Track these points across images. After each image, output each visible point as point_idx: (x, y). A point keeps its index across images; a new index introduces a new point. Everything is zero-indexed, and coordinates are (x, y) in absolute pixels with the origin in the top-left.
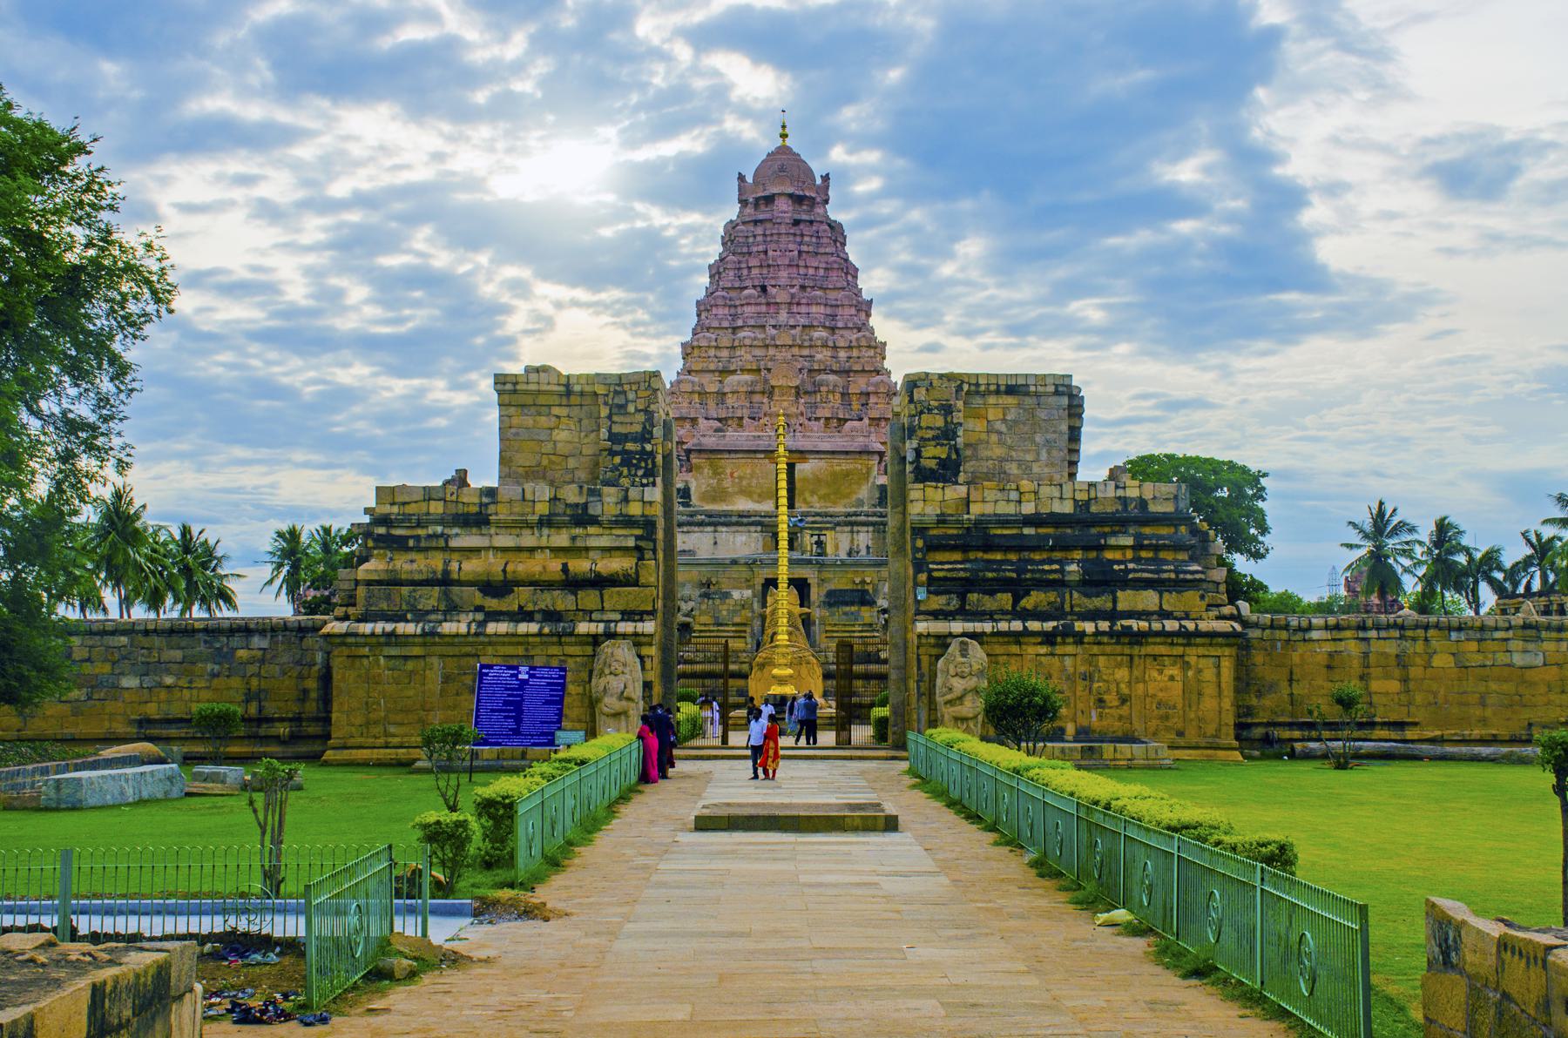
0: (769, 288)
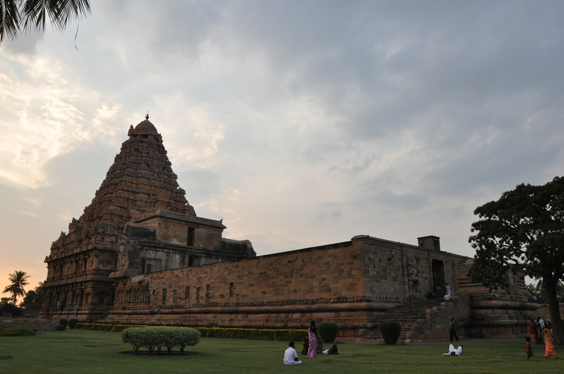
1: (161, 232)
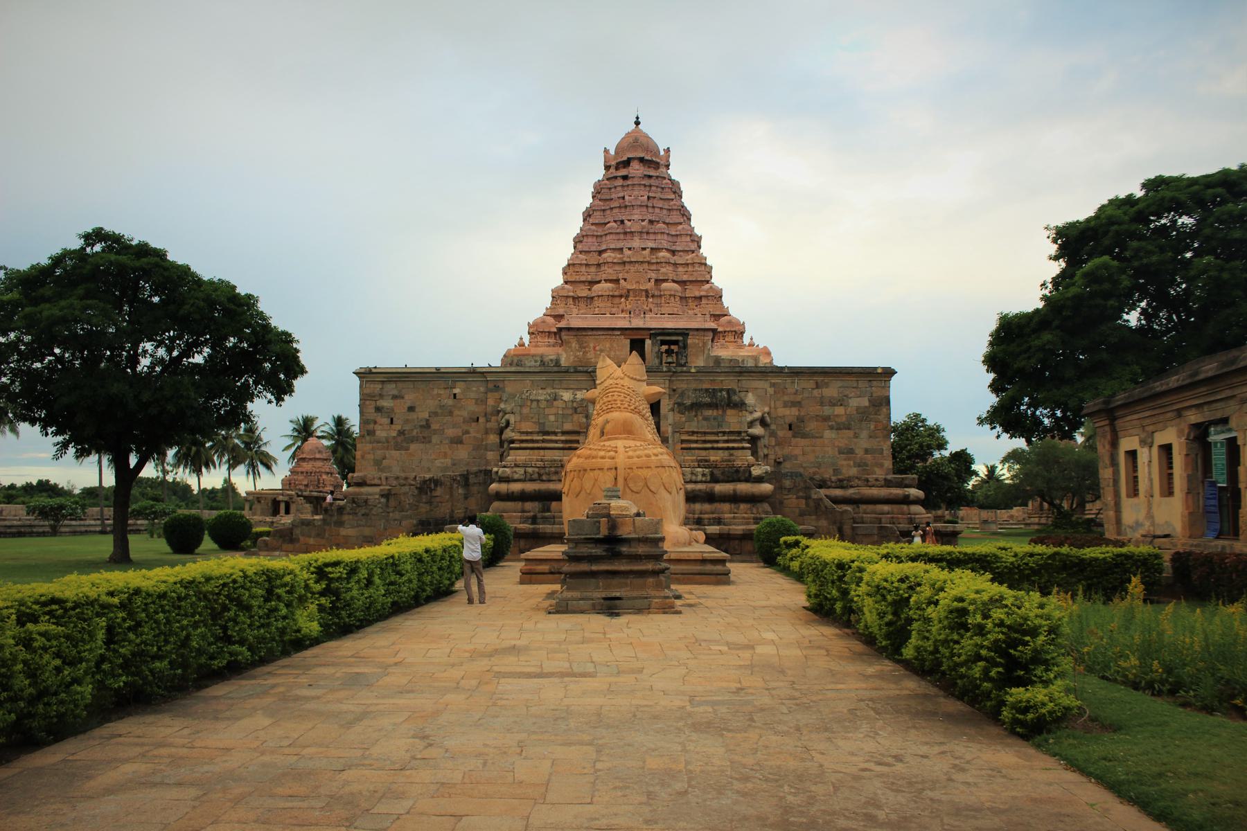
0: (626, 222)
1: (572, 358)
